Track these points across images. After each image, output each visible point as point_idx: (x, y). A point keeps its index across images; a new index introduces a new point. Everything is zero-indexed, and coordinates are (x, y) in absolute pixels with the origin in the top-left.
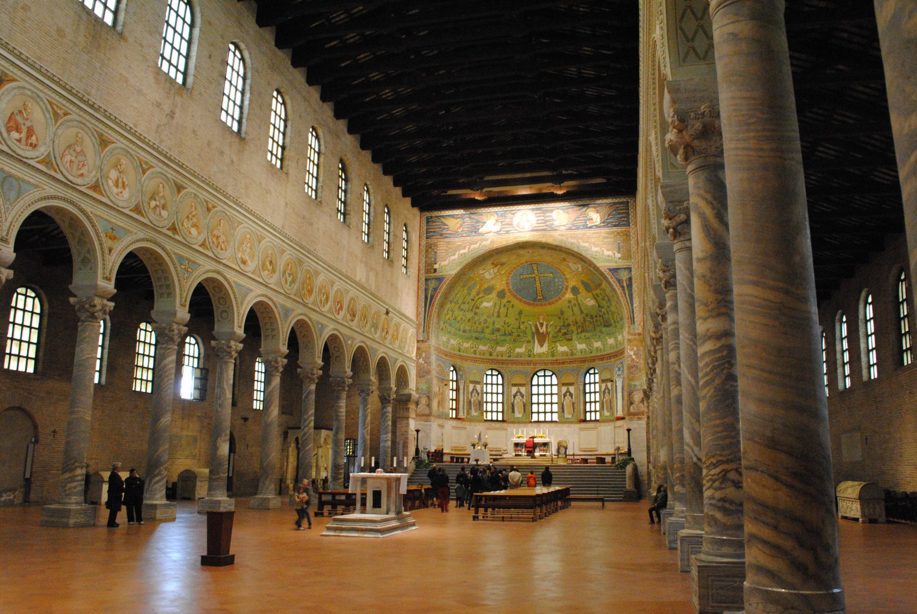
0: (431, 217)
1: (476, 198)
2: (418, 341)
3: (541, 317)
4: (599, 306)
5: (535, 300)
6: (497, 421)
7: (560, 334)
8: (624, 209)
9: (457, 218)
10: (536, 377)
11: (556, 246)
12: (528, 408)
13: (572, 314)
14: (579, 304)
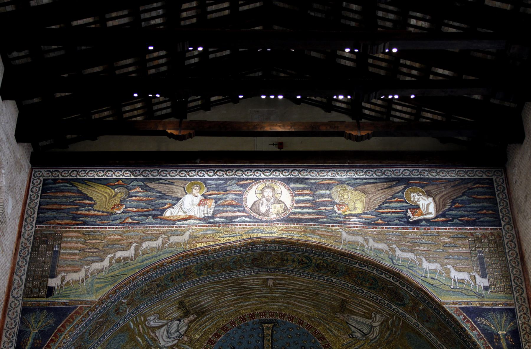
0: (55, 181)
1: (169, 131)
8: (485, 194)
9: (113, 187)
11: (343, 254)
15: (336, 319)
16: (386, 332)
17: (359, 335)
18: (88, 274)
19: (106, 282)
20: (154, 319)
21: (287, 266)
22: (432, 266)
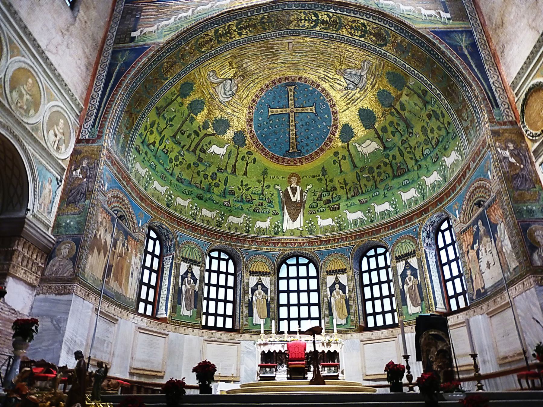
2: (78, 141)
3: (294, 180)
4: (385, 148)
5: (287, 153)
6: (224, 329)
7: (321, 203)
10: (284, 266)
12: (273, 309)
13: (339, 171)
14: (350, 155)
15: (336, 75)
16: (371, 78)
17: (352, 87)
18: (159, 27)
19: (171, 31)
20: (212, 76)
21: (302, 27)
22: (408, 8)
